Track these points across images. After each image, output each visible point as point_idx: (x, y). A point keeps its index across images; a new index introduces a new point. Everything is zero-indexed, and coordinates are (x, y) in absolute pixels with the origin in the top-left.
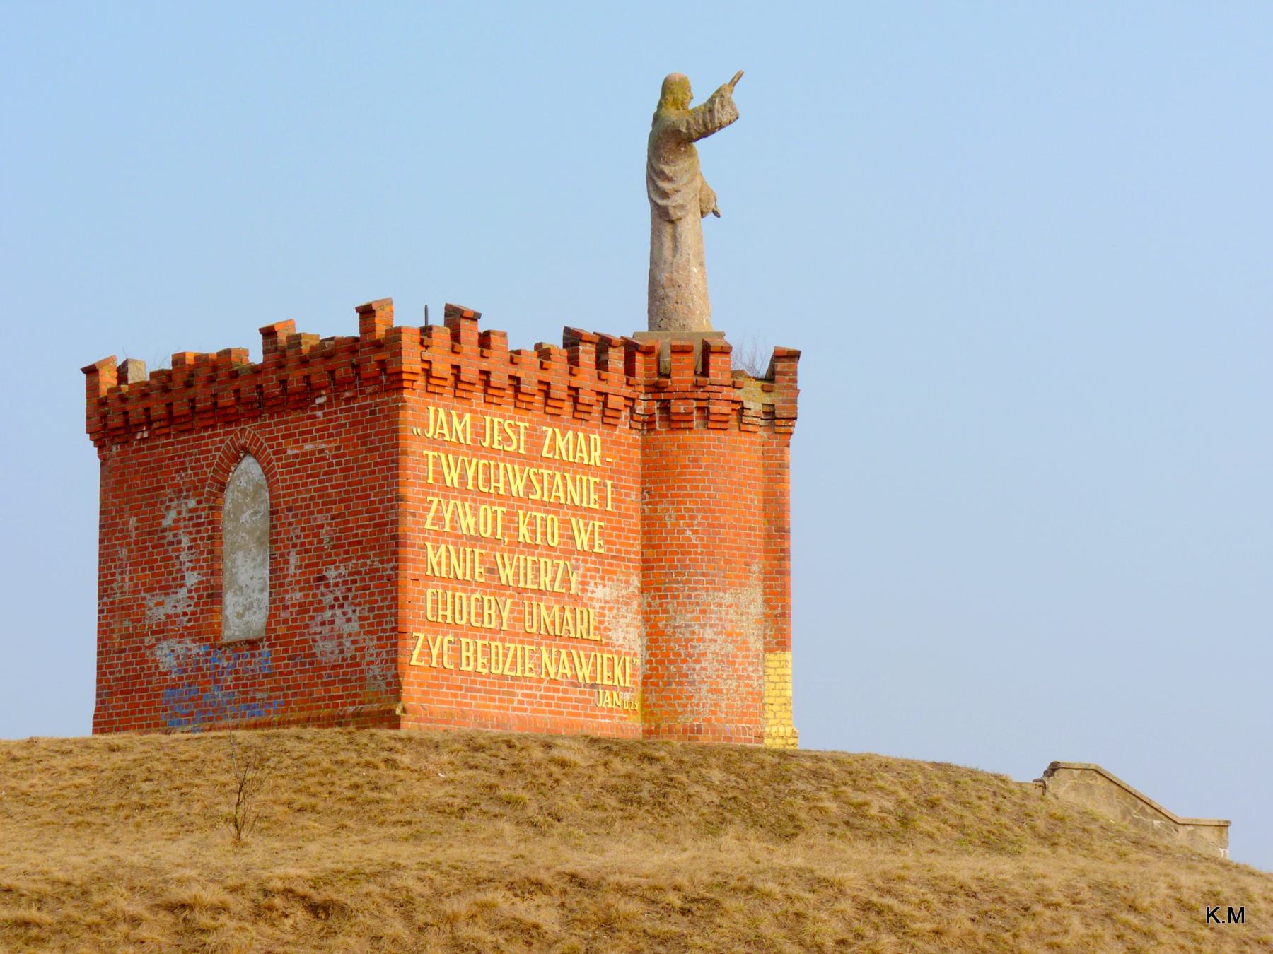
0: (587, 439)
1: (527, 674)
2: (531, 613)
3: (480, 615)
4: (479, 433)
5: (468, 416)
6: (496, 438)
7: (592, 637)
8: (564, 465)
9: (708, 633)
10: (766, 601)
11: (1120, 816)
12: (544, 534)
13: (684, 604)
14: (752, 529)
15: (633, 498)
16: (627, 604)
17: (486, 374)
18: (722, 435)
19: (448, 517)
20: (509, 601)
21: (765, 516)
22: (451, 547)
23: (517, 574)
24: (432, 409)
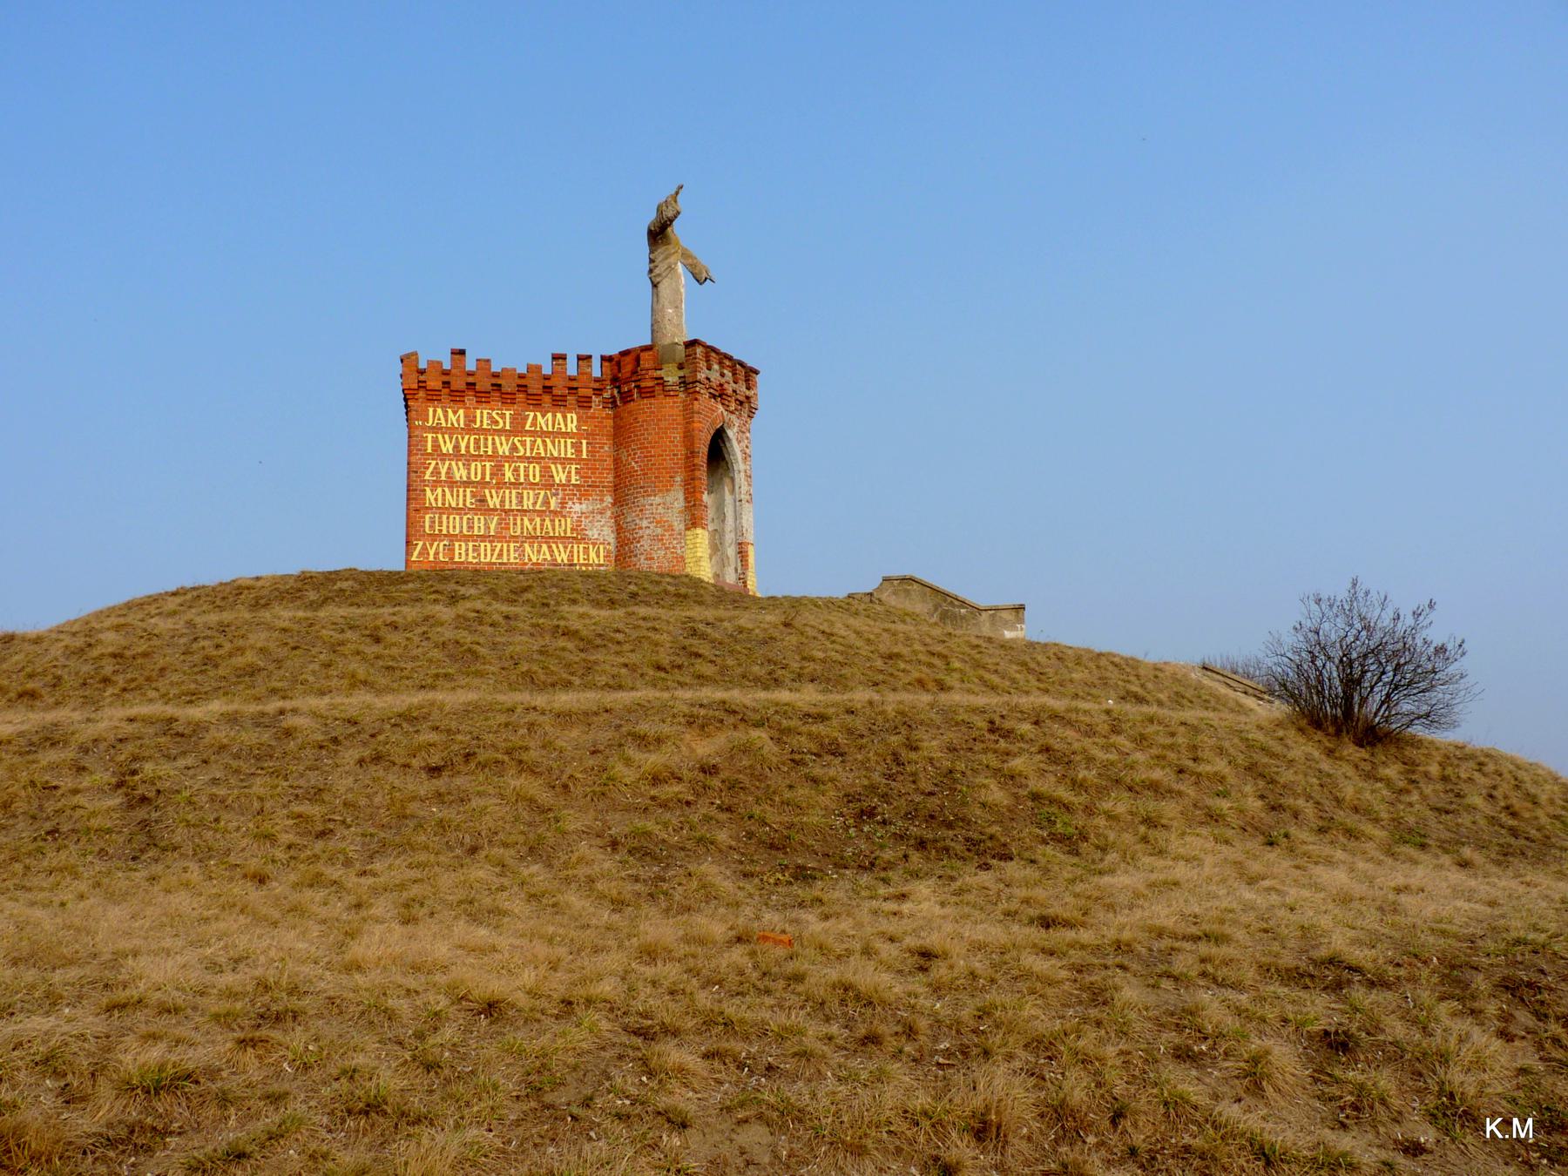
0: (565, 418)
1: (512, 561)
2: (515, 524)
3: (471, 528)
4: (470, 419)
5: (461, 412)
6: (485, 422)
7: (569, 534)
8: (544, 434)
9: (645, 523)
10: (686, 498)
11: (932, 609)
12: (527, 476)
13: (631, 508)
14: (674, 455)
15: (607, 449)
16: (601, 513)
17: (471, 385)
18: (652, 401)
19: (443, 471)
20: (496, 518)
21: (685, 446)
22: (446, 489)
23: (502, 502)
24: (431, 410)
